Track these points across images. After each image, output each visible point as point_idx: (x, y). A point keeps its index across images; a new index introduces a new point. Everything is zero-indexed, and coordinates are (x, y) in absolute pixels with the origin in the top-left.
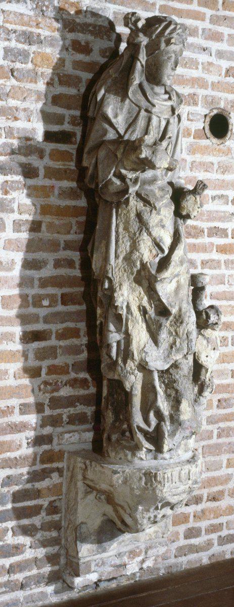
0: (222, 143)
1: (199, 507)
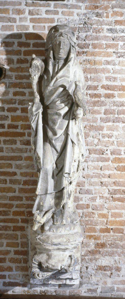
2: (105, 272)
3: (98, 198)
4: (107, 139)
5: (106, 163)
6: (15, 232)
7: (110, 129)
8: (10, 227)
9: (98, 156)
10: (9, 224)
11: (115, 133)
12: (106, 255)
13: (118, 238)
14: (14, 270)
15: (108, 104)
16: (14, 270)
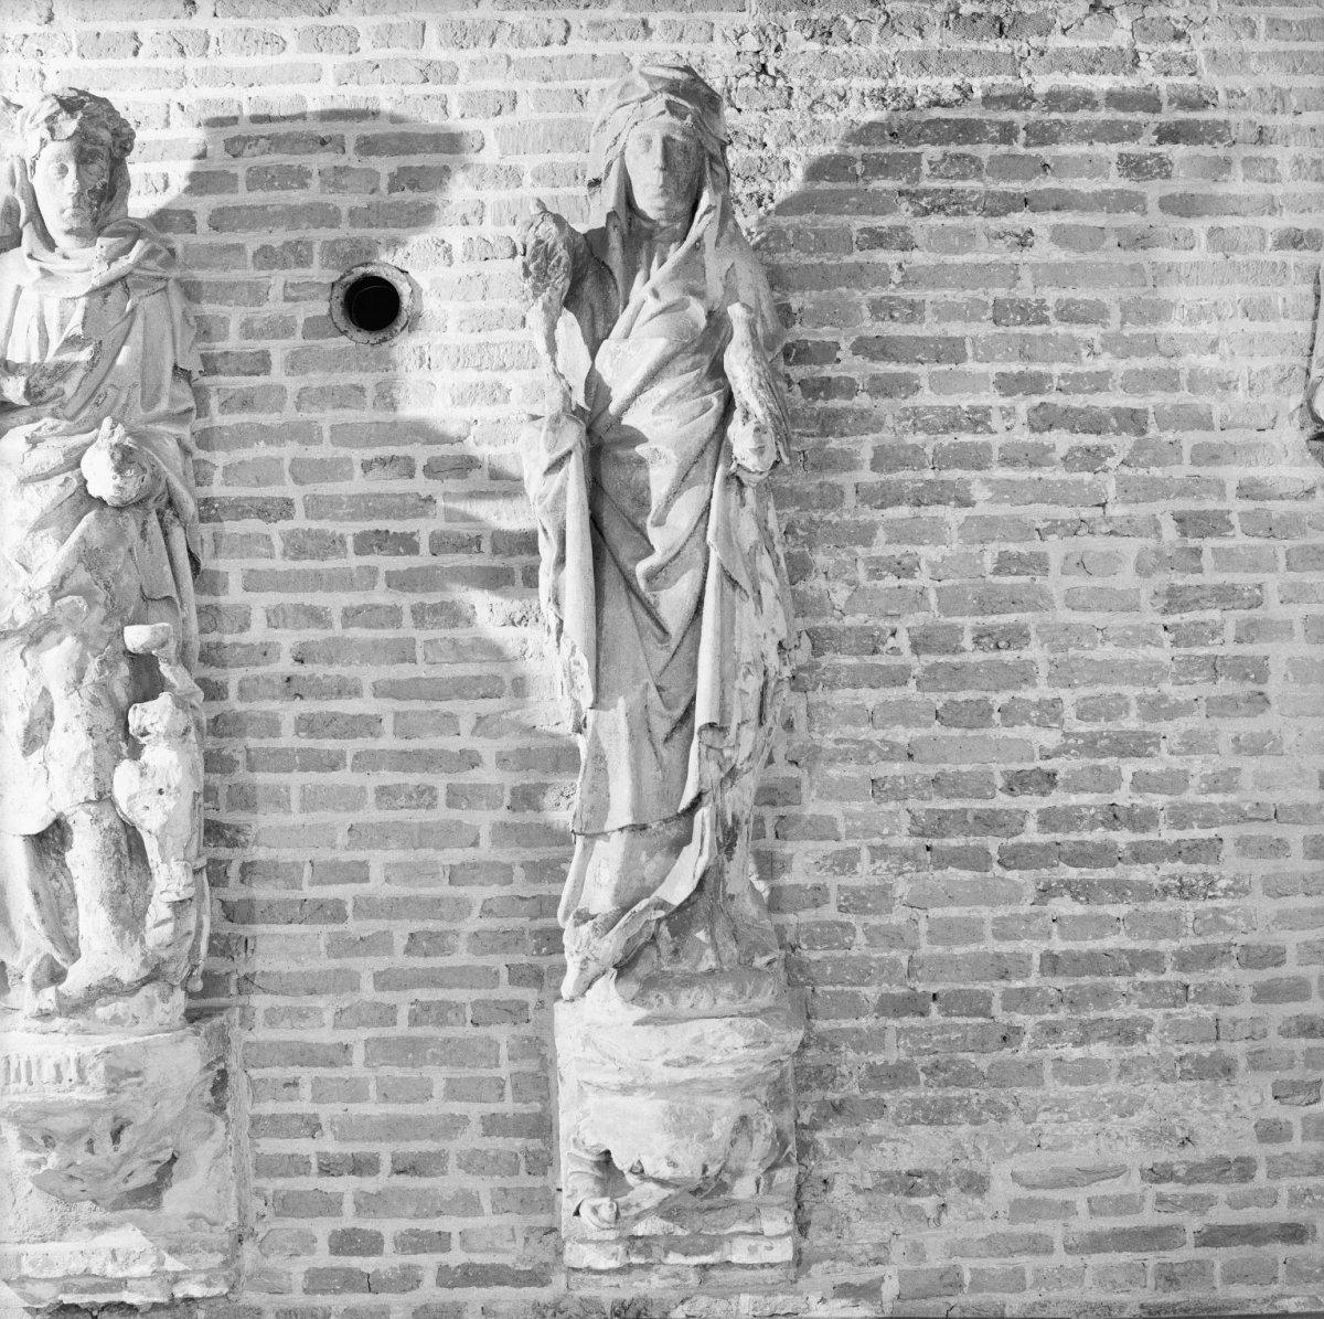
0: (385, 340)
1: (369, 1184)
2: (915, 1201)
3: (865, 854)
4: (890, 581)
5: (894, 694)
6: (481, 1031)
7: (899, 534)
8: (458, 1008)
9: (852, 661)
10: (456, 991)
11: (928, 553)
12: (914, 1121)
13: (965, 1038)
14: (487, 1208)
15: (889, 421)
16: (487, 1208)
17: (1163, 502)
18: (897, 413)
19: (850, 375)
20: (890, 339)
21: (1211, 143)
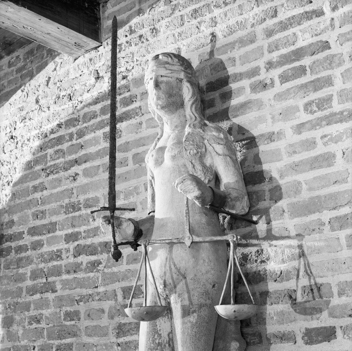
4: (35, 325)
11: (46, 312)
15: (35, 260)
17: (117, 283)
18: (37, 256)
19: (26, 243)
20: (37, 226)
21: (134, 117)
